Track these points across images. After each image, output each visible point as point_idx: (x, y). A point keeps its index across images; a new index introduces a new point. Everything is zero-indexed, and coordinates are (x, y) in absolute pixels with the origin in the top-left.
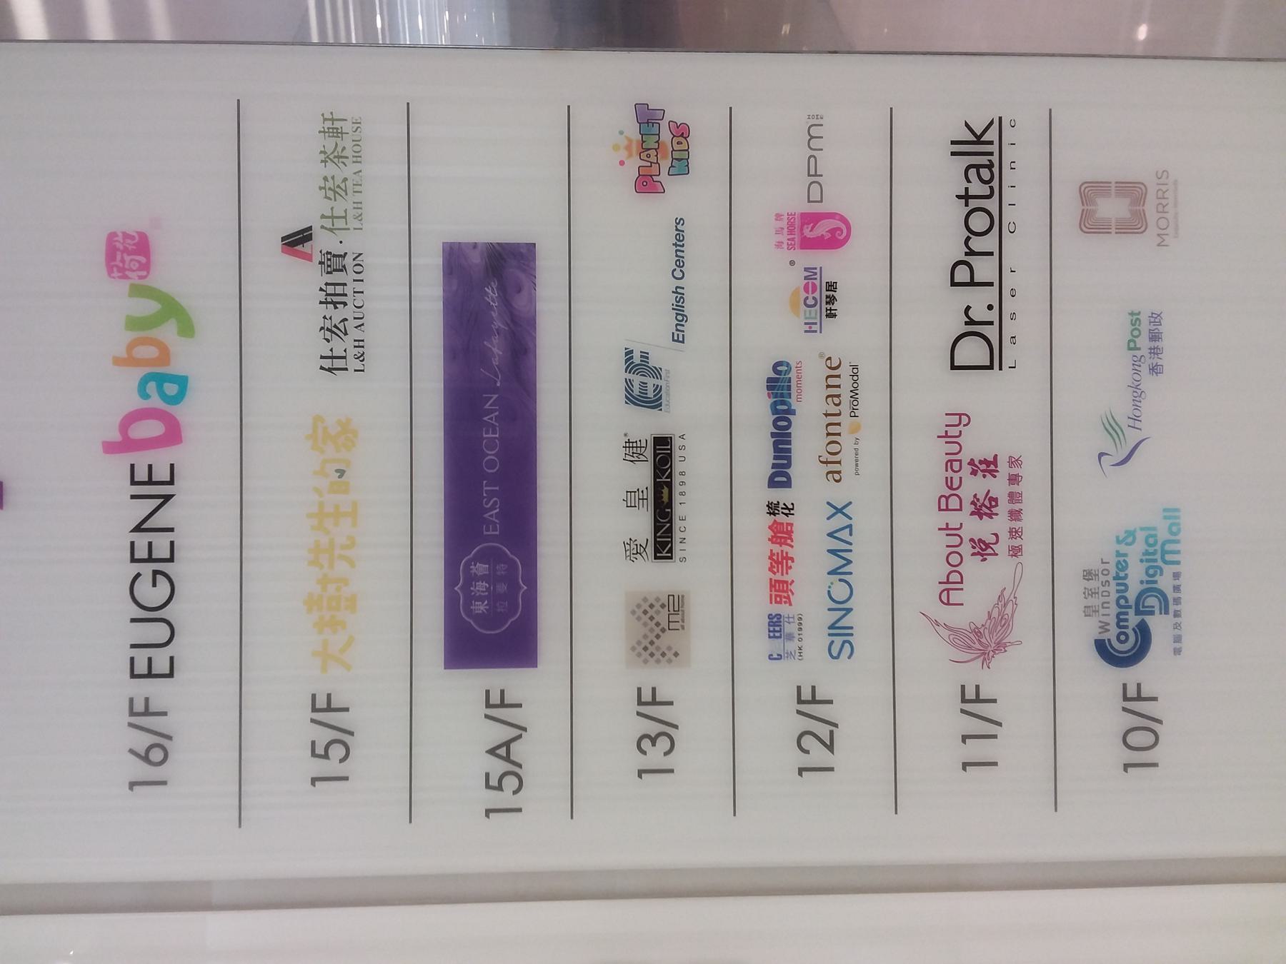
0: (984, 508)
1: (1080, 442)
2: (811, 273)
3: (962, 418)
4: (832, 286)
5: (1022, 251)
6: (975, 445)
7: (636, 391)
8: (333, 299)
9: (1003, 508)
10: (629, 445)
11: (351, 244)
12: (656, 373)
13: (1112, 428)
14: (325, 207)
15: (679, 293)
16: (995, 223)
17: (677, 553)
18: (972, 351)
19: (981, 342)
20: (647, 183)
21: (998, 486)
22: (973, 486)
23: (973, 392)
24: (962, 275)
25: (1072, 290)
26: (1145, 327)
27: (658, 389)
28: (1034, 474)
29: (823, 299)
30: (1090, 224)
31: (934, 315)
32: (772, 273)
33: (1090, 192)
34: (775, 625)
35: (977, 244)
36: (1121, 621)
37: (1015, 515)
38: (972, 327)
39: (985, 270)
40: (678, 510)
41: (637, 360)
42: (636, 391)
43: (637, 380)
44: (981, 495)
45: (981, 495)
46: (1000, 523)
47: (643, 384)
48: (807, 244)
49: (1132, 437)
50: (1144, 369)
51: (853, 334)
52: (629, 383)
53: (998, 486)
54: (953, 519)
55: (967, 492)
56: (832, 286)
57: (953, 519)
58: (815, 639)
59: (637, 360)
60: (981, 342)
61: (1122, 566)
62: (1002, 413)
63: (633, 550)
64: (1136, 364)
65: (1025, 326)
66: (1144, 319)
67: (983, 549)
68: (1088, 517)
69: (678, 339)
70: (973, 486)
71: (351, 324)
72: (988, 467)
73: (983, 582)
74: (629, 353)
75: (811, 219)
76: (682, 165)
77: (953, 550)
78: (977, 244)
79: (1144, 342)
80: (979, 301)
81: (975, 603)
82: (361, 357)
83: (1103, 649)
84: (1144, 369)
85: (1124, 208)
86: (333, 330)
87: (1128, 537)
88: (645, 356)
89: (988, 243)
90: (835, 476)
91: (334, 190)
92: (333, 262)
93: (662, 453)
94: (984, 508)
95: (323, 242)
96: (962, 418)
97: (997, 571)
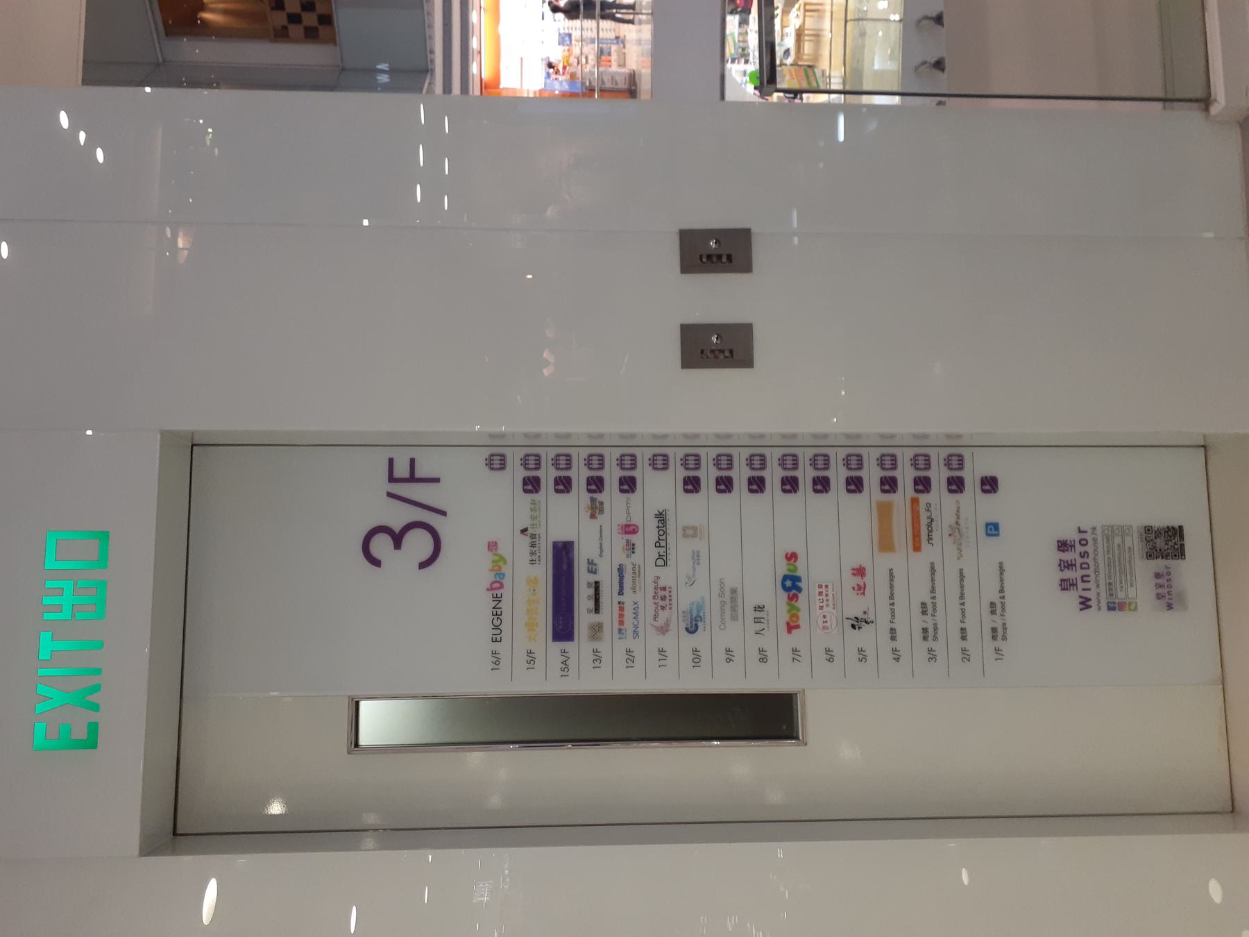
2: (628, 542)
5: (671, 539)
6: (661, 583)
8: (533, 546)
11: (537, 531)
16: (665, 533)
18: (660, 562)
19: (662, 560)
20: (593, 516)
21: (666, 593)
22: (661, 593)
23: (660, 572)
24: (658, 544)
29: (631, 548)
31: (652, 553)
32: (620, 541)
34: (620, 630)
39: (663, 543)
40: (601, 600)
44: (663, 596)
46: (667, 602)
47: (592, 568)
48: (627, 533)
51: (637, 558)
53: (666, 593)
58: (630, 633)
60: (662, 560)
63: (589, 611)
67: (663, 608)
70: (661, 593)
72: (664, 589)
73: (663, 615)
76: (602, 511)
80: (662, 550)
81: (661, 621)
86: (532, 554)
91: (533, 518)
92: (533, 536)
93: (597, 585)
94: (663, 598)
95: (530, 531)
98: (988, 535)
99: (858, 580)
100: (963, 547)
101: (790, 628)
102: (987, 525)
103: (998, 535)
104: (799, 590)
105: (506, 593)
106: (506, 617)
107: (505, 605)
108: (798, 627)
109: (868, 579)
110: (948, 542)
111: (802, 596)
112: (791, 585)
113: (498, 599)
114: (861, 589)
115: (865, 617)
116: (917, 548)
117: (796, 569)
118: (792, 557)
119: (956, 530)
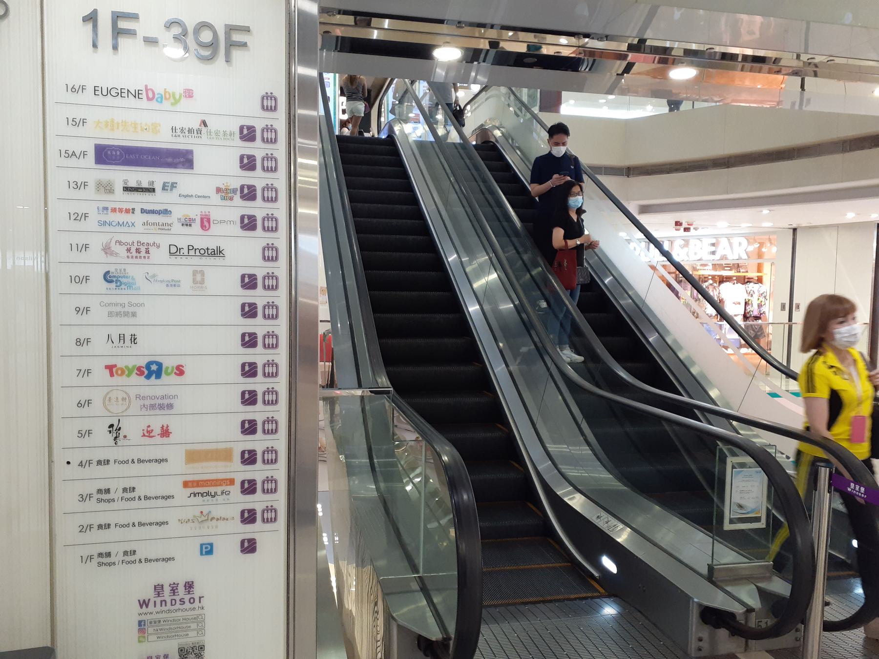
0: (138, 251)
1: (152, 270)
3: (158, 247)
4: (190, 225)
5: (197, 260)
6: (152, 250)
8: (190, 131)
9: (138, 255)
11: (204, 135)
12: (171, 190)
13: (154, 276)
14: (213, 131)
16: (202, 255)
18: (173, 250)
19: (175, 252)
20: (218, 190)
21: (143, 254)
22: (143, 249)
23: (165, 249)
24: (190, 248)
25: (182, 271)
28: (146, 261)
29: (187, 223)
30: (195, 273)
31: (183, 243)
32: (195, 213)
33: (202, 273)
34: (107, 209)
35: (197, 251)
36: (114, 277)
37: (136, 257)
38: (179, 250)
39: (192, 253)
40: (136, 193)
44: (141, 251)
45: (141, 251)
46: (134, 254)
48: (202, 220)
49: (152, 280)
51: (177, 228)
53: (143, 254)
54: (135, 244)
55: (141, 247)
56: (190, 225)
57: (135, 244)
58: (103, 218)
60: (175, 252)
61: (127, 277)
62: (159, 255)
63: (125, 182)
65: (179, 260)
67: (129, 250)
68: (136, 271)
70: (143, 249)
72: (147, 252)
73: (122, 250)
75: (209, 221)
76: (223, 198)
77: (128, 244)
78: (197, 251)
80: (185, 251)
81: (116, 248)
83: (108, 272)
85: (199, 279)
86: (182, 130)
87: (133, 278)
89: (198, 253)
90: (144, 224)
91: (217, 133)
92: (199, 131)
94: (138, 251)
95: (204, 129)
96: (158, 247)
97: (125, 254)
99: (157, 431)
101: (111, 369)
104: (148, 377)
105: (144, 103)
106: (118, 101)
107: (131, 101)
108: (112, 375)
109: (158, 440)
111: (142, 380)
112: (153, 370)
113: (137, 95)
114: (148, 433)
115: (121, 436)
116: (186, 484)
117: (168, 374)
118: (180, 371)
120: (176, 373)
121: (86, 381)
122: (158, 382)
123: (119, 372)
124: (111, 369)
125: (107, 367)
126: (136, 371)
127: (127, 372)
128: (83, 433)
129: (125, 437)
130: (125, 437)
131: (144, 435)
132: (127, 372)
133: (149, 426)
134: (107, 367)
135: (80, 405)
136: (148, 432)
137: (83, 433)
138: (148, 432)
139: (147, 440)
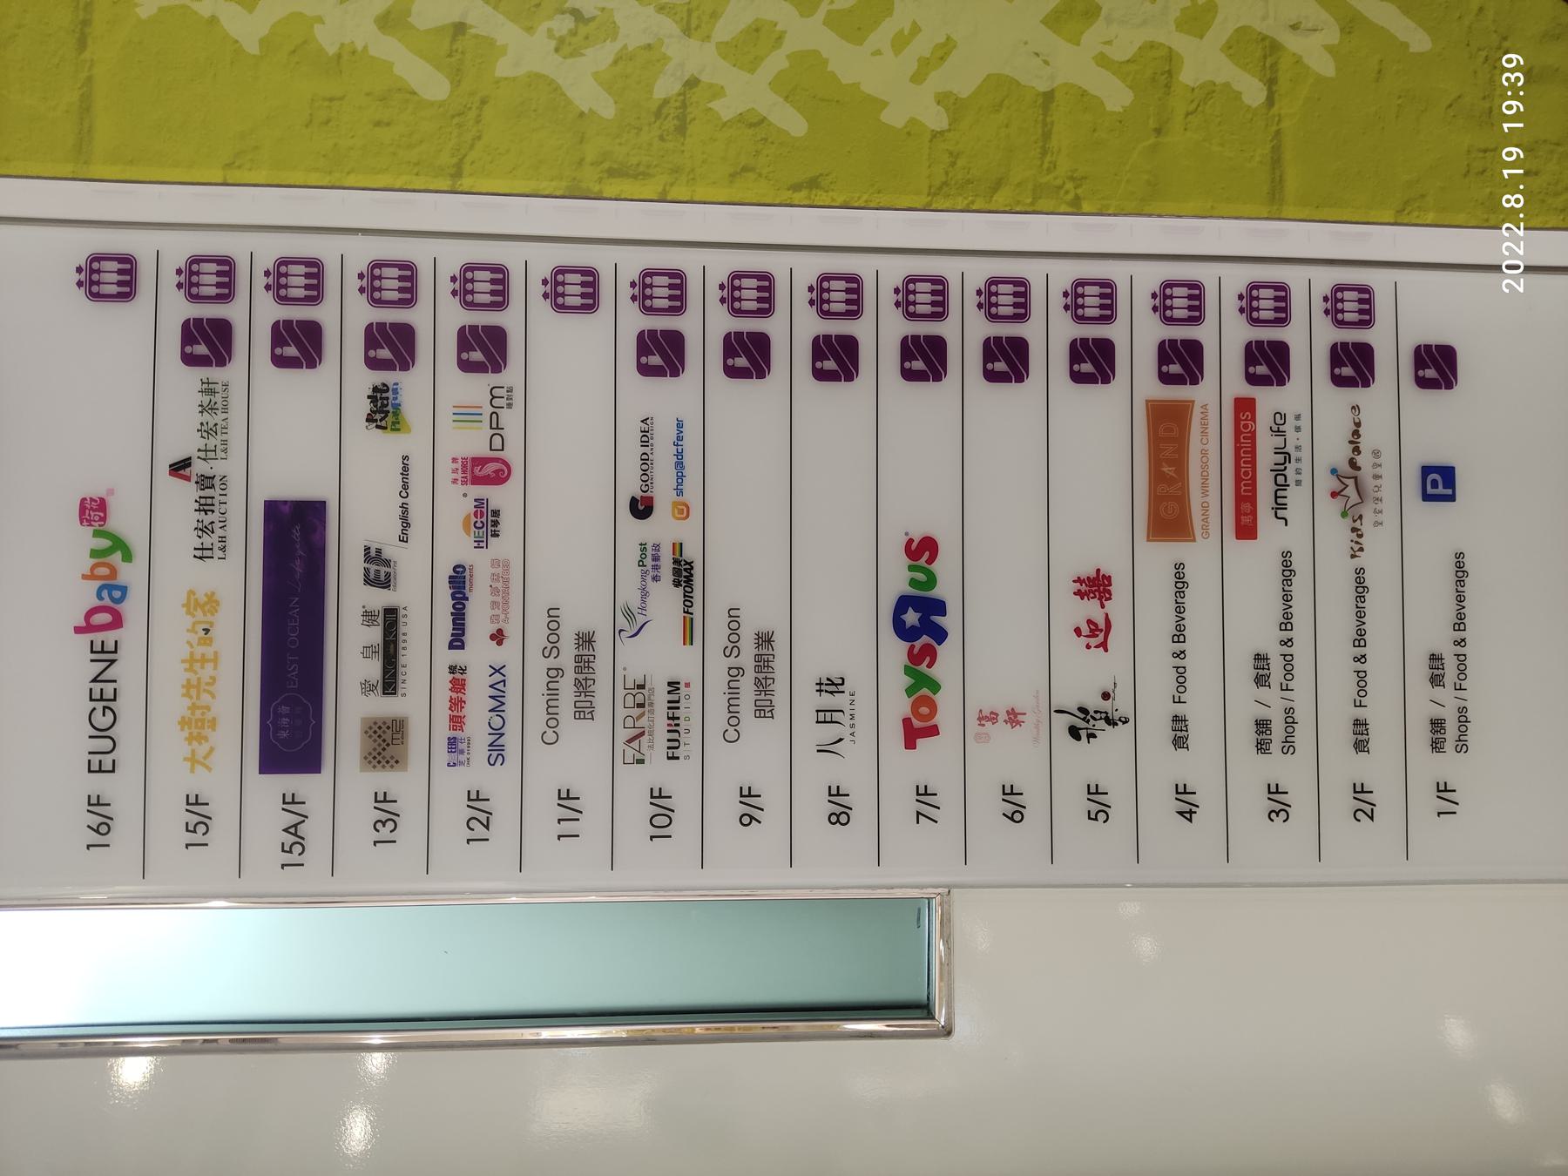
7: (372, 576)
10: (366, 614)
12: (387, 563)
15: (405, 508)
17: (400, 691)
26: (649, 552)
27: (388, 575)
34: (452, 743)
41: (373, 553)
42: (372, 576)
43: (373, 568)
47: (379, 571)
50: (649, 578)
52: (367, 570)
59: (373, 553)
64: (644, 574)
66: (649, 547)
69: (404, 539)
71: (217, 526)
74: (367, 549)
79: (649, 562)
82: (223, 549)
84: (649, 578)
88: (379, 551)
98: (1426, 497)
99: (1091, 609)
100: (1366, 527)
101: (916, 732)
102: (1426, 470)
103: (1452, 498)
104: (941, 635)
105: (130, 638)
106: (129, 706)
107: (127, 670)
108: (933, 731)
109: (1118, 608)
110: (1329, 510)
111: (947, 653)
112: (920, 621)
113: (106, 656)
114: (1097, 633)
115: (1106, 705)
116: (1246, 530)
117: (932, 581)
118: (922, 550)
119: (1351, 484)
120: (931, 561)
121: (948, 798)
122: (953, 607)
123: (924, 710)
124: (916, 732)
125: (910, 744)
126: (923, 667)
127: (925, 691)
128: (1094, 807)
129: (1106, 696)
130: (1106, 696)
131: (1104, 645)
132: (925, 691)
133: (1078, 631)
134: (910, 744)
135: (1016, 816)
136: (1093, 634)
137: (1094, 807)
138: (1093, 634)
139: (1119, 638)
